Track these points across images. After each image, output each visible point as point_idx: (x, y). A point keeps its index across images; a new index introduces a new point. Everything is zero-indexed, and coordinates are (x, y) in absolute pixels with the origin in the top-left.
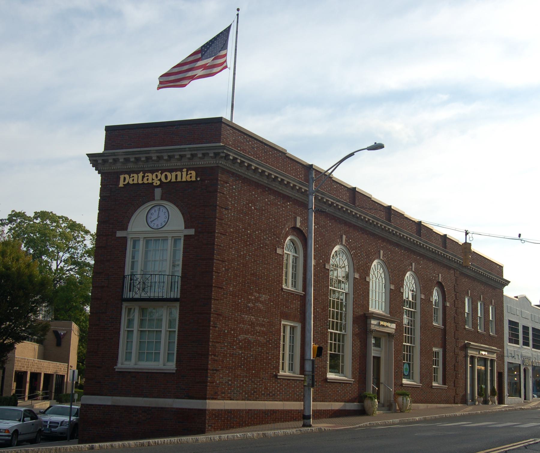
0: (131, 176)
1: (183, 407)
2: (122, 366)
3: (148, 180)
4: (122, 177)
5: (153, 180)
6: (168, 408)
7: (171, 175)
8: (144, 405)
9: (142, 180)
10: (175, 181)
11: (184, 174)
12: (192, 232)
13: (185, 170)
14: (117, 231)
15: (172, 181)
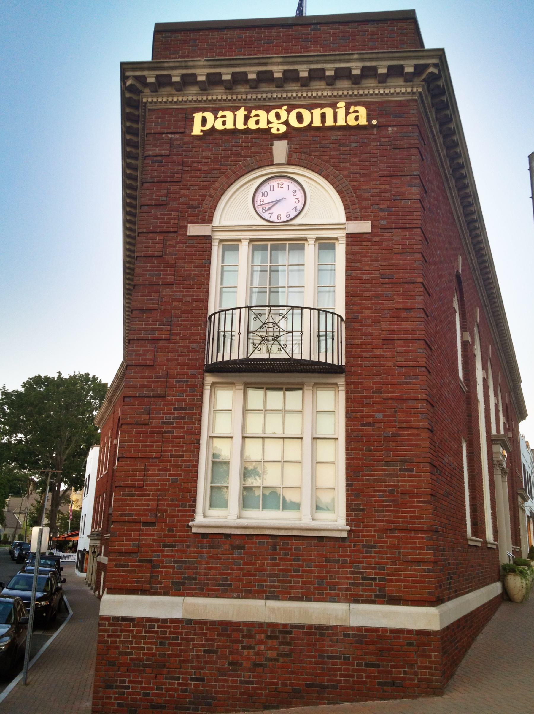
0: (219, 115)
1: (377, 626)
2: (206, 520)
3: (257, 122)
4: (198, 117)
5: (269, 122)
6: (334, 628)
7: (312, 114)
8: (272, 620)
9: (245, 123)
10: (321, 125)
11: (341, 112)
12: (365, 227)
13: (341, 104)
14: (189, 225)
15: (313, 125)
